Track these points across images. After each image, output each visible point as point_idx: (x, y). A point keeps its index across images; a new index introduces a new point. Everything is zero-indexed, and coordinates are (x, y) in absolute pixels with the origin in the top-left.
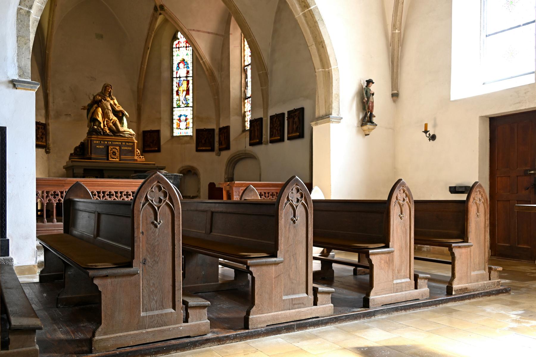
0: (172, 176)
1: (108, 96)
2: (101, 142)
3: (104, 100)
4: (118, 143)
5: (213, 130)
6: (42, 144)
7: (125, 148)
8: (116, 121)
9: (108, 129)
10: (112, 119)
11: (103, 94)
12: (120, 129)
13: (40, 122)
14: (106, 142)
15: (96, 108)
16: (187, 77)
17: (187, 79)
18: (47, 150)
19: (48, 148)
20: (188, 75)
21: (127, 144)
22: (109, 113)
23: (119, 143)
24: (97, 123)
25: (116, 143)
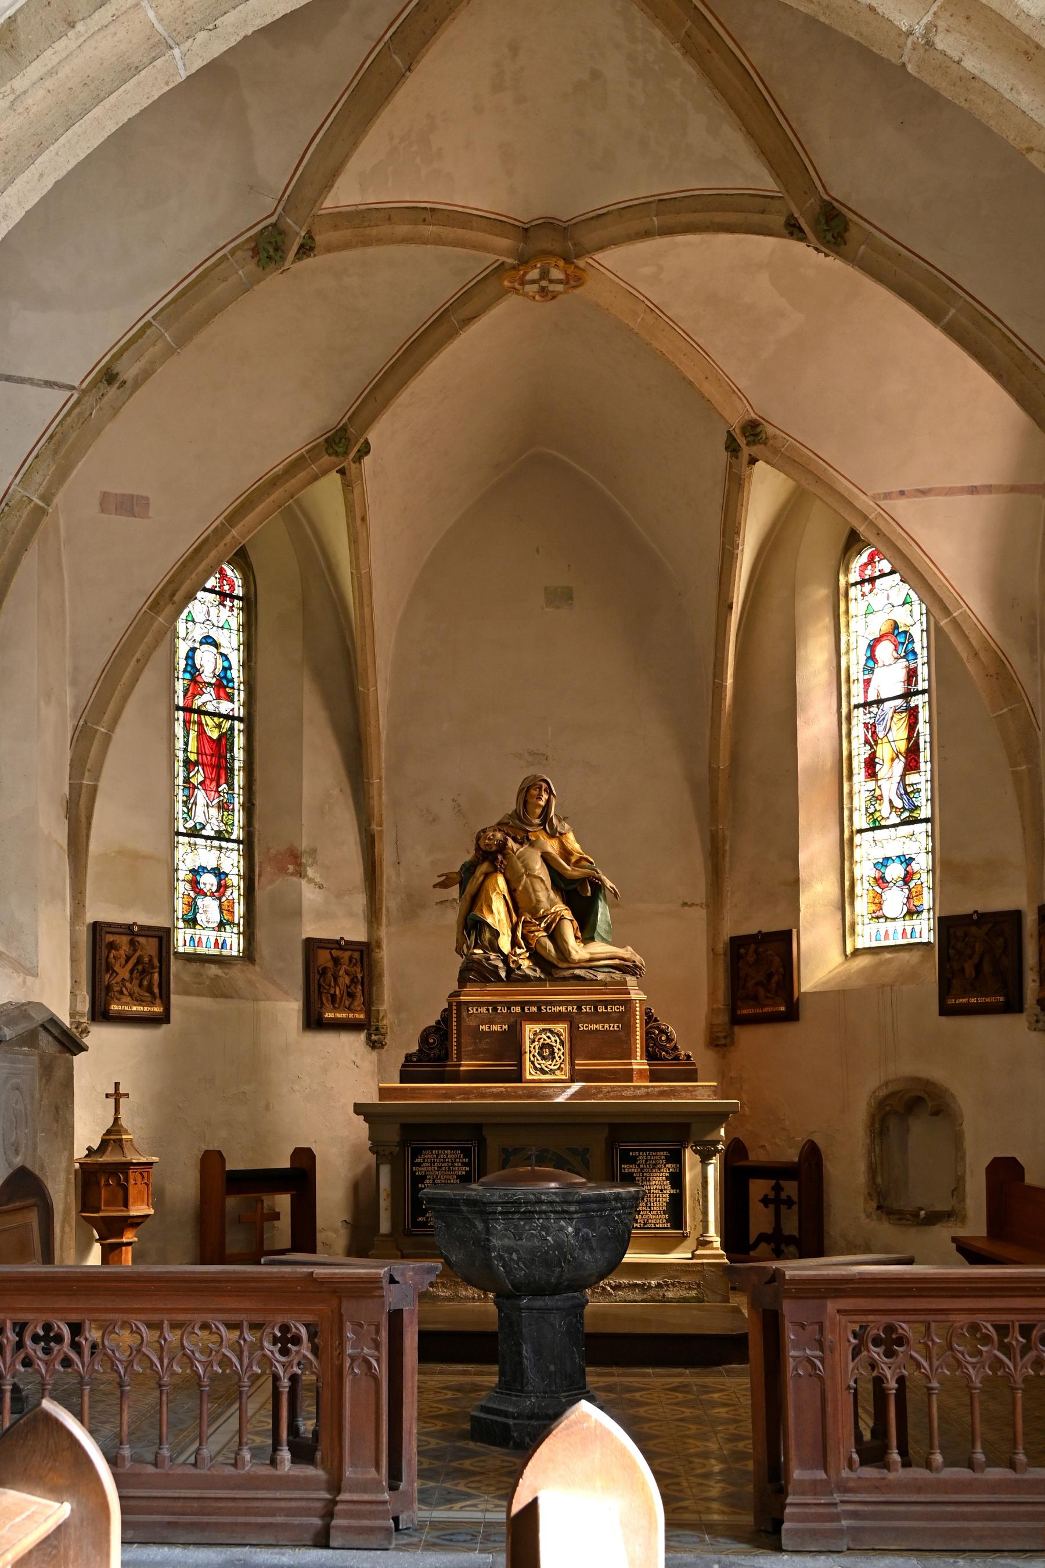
0: (570, 1203)
1: (540, 825)
2: (495, 1009)
3: (515, 840)
5: (1016, 916)
6: (351, 1016)
7: (594, 1027)
8: (562, 918)
9: (528, 954)
10: (544, 917)
11: (520, 819)
12: (573, 952)
13: (342, 938)
14: (518, 1009)
15: (487, 875)
16: (907, 695)
17: (908, 703)
18: (374, 1037)
19: (377, 1029)
20: (913, 689)
21: (601, 1009)
22: (535, 891)
23: (570, 1008)
24: (487, 935)
25: (557, 1009)
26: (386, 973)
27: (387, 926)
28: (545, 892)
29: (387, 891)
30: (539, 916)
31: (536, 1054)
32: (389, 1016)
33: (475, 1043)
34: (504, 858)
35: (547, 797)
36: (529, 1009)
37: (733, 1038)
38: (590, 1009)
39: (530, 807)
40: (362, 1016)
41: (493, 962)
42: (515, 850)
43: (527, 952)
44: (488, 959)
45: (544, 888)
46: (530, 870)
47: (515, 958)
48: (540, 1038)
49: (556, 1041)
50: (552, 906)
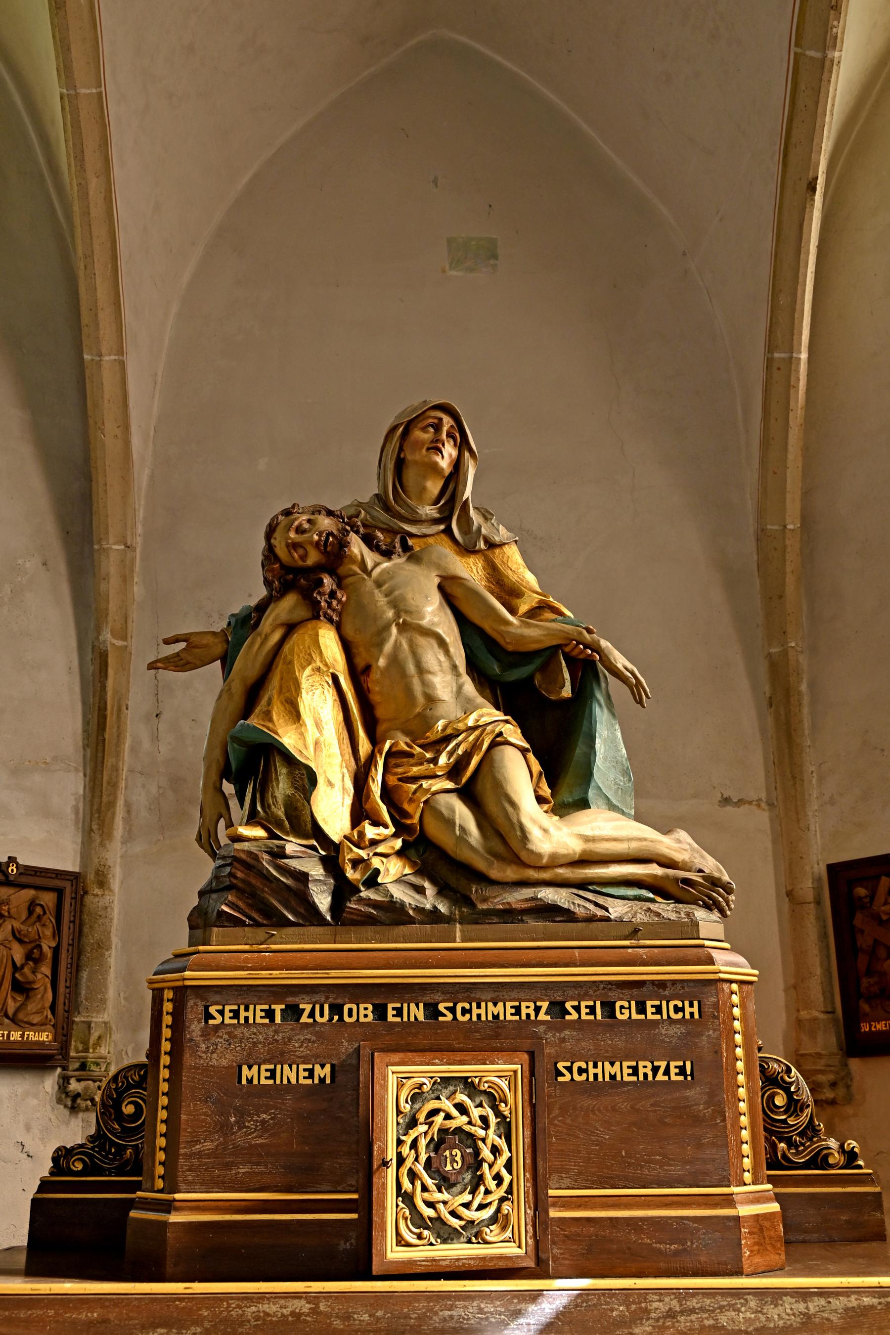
1: (436, 521)
2: (293, 1012)
3: (369, 540)
4: (505, 1010)
6: (16, 1036)
8: (499, 741)
9: (398, 844)
10: (446, 739)
11: (387, 508)
12: (535, 833)
13: (12, 859)
14: (366, 1012)
15: (290, 628)
19: (83, 1067)
22: (421, 670)
23: (527, 1009)
25: (488, 1011)
26: (115, 940)
27: (124, 843)
28: (449, 677)
29: (131, 771)
30: (432, 736)
31: (420, 1168)
32: (116, 1036)
33: (224, 1128)
34: (339, 586)
35: (455, 453)
36: (399, 1012)
37: (848, 1087)
38: (592, 1010)
39: (410, 475)
40: (45, 1037)
41: (293, 864)
42: (370, 565)
43: (395, 835)
44: (279, 854)
45: (446, 664)
46: (407, 612)
47: (363, 854)
48: (434, 1112)
49: (484, 1119)
50: (467, 712)
